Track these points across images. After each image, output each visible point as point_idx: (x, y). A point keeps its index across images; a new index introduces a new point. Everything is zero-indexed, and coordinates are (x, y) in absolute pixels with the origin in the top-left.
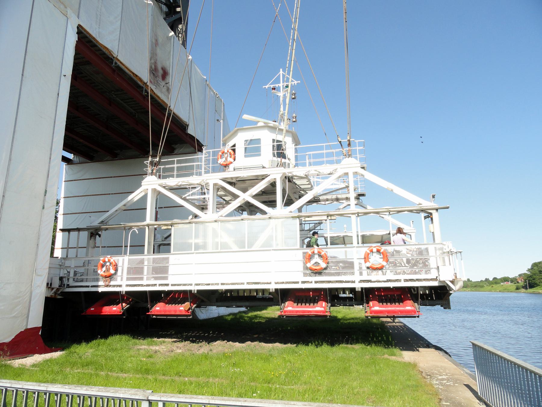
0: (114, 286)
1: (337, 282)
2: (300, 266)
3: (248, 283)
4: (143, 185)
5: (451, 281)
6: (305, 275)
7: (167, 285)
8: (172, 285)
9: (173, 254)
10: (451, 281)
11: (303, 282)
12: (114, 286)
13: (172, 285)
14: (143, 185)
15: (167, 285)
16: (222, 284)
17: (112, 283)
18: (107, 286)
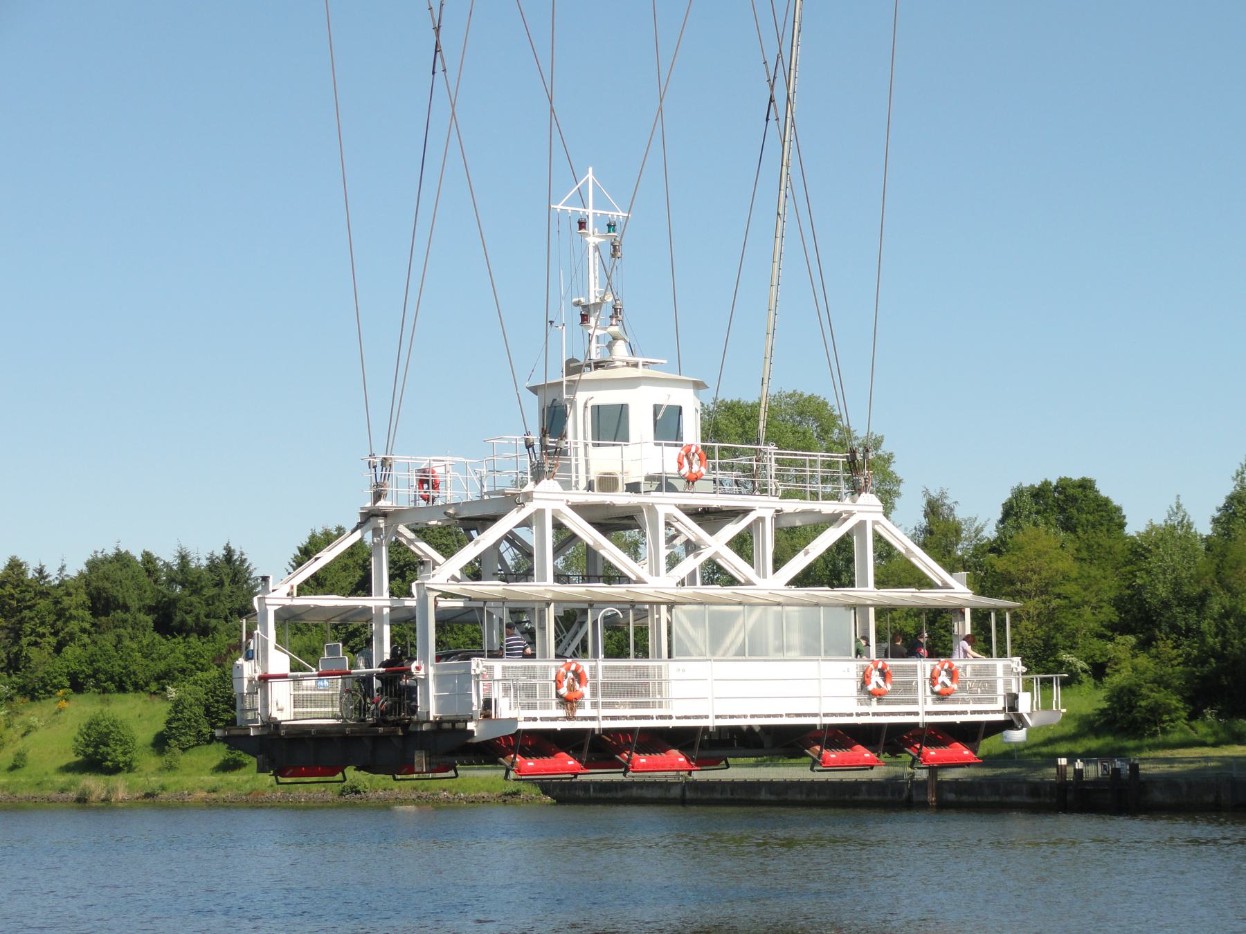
0: (585, 718)
1: (632, 718)
2: (853, 687)
3: (788, 715)
4: (537, 499)
5: (1028, 714)
6: (860, 702)
7: (670, 717)
8: (678, 718)
9: (675, 661)
10: (1028, 714)
11: (858, 715)
12: (585, 718)
13: (678, 718)
14: (537, 499)
15: (670, 717)
16: (753, 716)
17: (579, 713)
18: (568, 718)
